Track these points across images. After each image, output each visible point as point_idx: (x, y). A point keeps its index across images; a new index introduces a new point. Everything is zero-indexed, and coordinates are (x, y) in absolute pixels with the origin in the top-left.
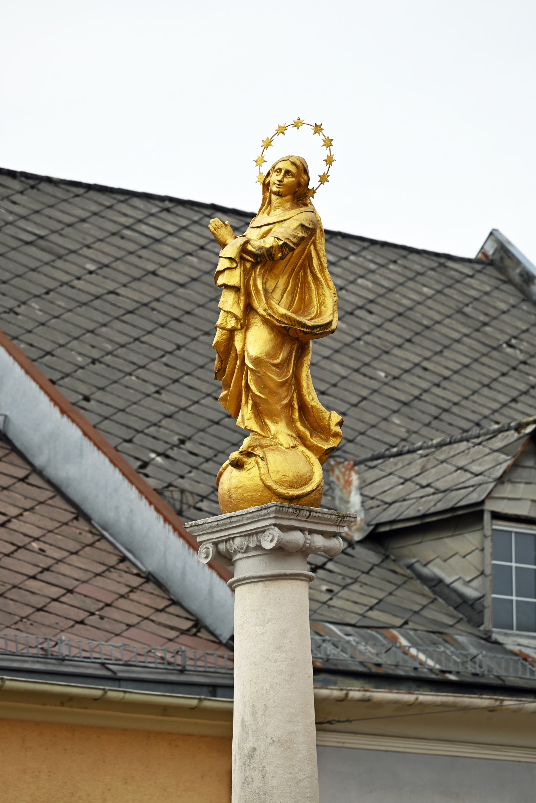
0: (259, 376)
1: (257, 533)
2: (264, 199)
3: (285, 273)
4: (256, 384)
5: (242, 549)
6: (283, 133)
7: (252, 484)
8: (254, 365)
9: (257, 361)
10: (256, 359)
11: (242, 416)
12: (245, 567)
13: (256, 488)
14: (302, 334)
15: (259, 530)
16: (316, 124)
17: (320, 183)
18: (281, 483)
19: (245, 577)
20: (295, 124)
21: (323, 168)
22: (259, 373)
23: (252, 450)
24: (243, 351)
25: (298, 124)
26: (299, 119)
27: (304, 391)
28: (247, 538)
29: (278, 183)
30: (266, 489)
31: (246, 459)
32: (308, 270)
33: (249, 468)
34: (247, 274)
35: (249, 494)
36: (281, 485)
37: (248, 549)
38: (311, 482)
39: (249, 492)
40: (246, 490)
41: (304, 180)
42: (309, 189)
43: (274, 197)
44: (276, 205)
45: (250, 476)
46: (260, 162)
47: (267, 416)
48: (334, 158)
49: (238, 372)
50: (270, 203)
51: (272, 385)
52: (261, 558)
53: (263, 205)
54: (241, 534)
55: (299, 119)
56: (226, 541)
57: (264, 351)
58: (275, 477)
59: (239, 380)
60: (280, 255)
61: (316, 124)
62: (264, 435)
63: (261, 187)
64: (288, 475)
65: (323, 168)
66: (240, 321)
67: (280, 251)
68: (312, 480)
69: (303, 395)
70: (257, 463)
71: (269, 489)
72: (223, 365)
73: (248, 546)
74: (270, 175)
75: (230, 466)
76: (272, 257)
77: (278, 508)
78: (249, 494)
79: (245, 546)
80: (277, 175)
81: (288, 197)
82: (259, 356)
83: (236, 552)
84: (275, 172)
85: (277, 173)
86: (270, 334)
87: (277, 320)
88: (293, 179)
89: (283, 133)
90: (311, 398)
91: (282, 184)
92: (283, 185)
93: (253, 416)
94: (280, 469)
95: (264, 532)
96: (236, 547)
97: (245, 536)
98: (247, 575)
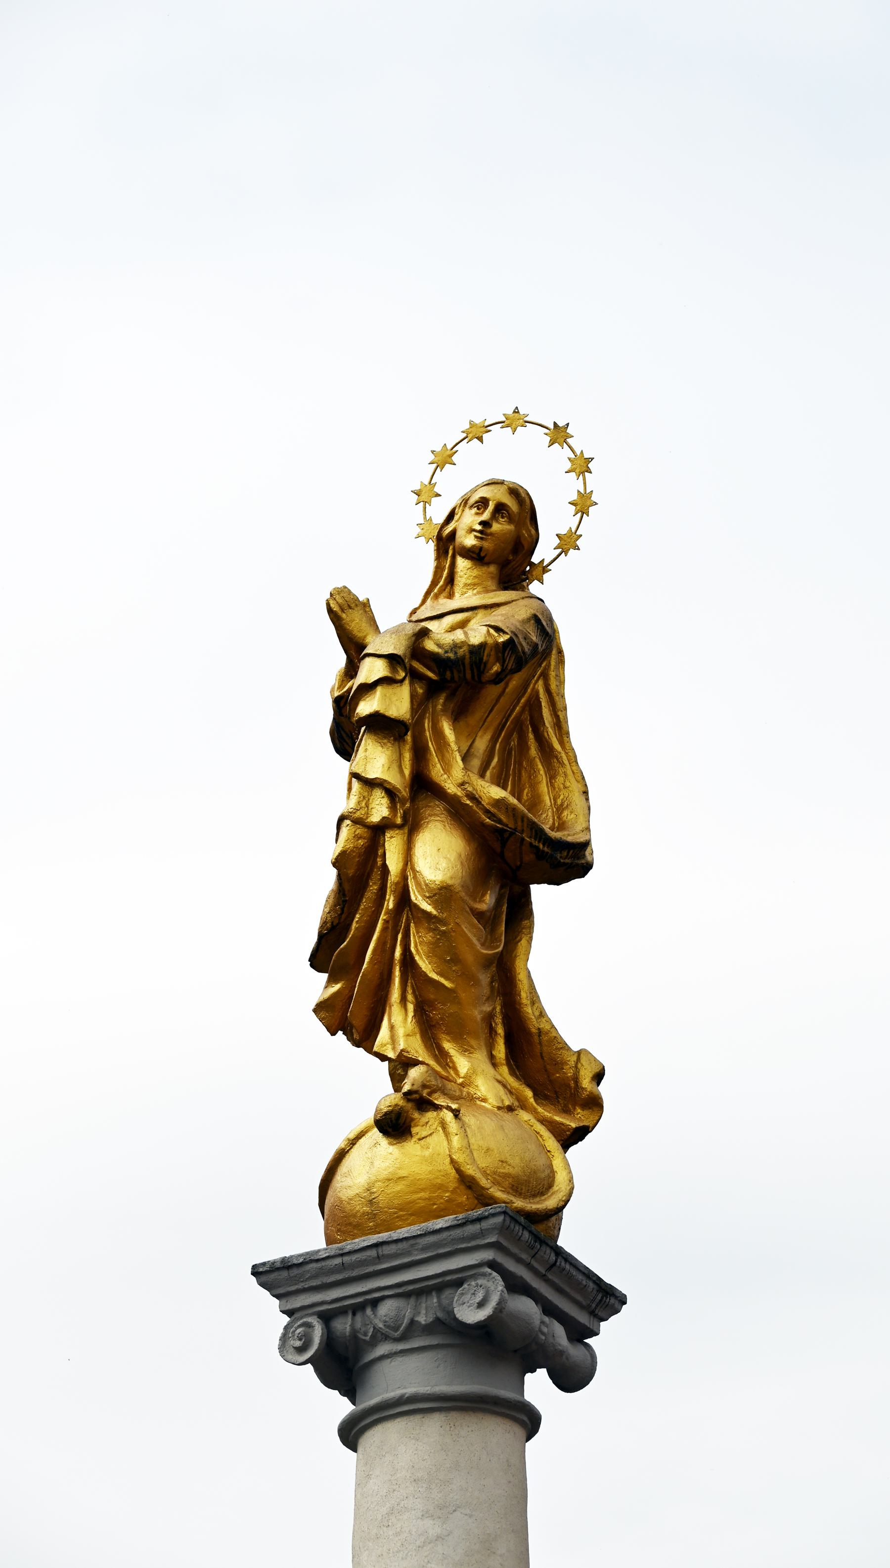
0: (444, 932)
1: (439, 1289)
2: (438, 570)
3: (487, 728)
4: (434, 952)
5: (396, 1329)
6: (480, 439)
7: (430, 1172)
8: (435, 904)
9: (442, 895)
11: (392, 1027)
12: (400, 1374)
13: (439, 1181)
14: (532, 857)
15: (448, 1278)
16: (555, 424)
17: (559, 550)
18: (499, 1179)
19: (402, 1396)
20: (507, 422)
21: (567, 520)
22: (445, 925)
23: (430, 1094)
24: (404, 877)
25: (515, 420)
26: (516, 411)
27: (523, 995)
28: (412, 1300)
29: (479, 528)
30: (462, 1187)
31: (416, 1115)
32: (531, 736)
33: (424, 1134)
34: (418, 705)
35: (422, 1194)
36: (495, 1183)
37: (412, 1329)
38: (551, 1191)
39: (422, 1190)
40: (415, 1185)
41: (530, 535)
42: (532, 565)
43: (462, 564)
44: (469, 582)
45: (427, 1153)
46: (425, 495)
47: (447, 1034)
48: (594, 498)
49: (384, 930)
50: (451, 580)
51: (469, 958)
52: (440, 1354)
53: (434, 583)
54: (400, 1290)
55: (516, 411)
56: (357, 1309)
58: (484, 1162)
59: (385, 949)
60: (496, 668)
61: (555, 424)
62: (444, 1073)
63: (432, 546)
64: (511, 1161)
65: (567, 520)
66: (403, 804)
67: (497, 660)
68: (555, 1188)
69: (520, 1004)
70: (443, 1125)
71: (469, 1187)
72: (344, 916)
73: (412, 1322)
74: (456, 517)
75: (376, 1129)
78: (422, 1194)
79: (406, 1321)
80: (477, 514)
81: (492, 568)
82: (450, 882)
83: (380, 1336)
84: (471, 507)
85: (475, 510)
86: (469, 845)
87: (487, 812)
88: (511, 527)
89: (480, 439)
90: (537, 1013)
91: (489, 531)
92: (491, 534)
93: (417, 1030)
94: (493, 1145)
95: (459, 1283)
96: (381, 1325)
97: (407, 1295)
98: (410, 1390)
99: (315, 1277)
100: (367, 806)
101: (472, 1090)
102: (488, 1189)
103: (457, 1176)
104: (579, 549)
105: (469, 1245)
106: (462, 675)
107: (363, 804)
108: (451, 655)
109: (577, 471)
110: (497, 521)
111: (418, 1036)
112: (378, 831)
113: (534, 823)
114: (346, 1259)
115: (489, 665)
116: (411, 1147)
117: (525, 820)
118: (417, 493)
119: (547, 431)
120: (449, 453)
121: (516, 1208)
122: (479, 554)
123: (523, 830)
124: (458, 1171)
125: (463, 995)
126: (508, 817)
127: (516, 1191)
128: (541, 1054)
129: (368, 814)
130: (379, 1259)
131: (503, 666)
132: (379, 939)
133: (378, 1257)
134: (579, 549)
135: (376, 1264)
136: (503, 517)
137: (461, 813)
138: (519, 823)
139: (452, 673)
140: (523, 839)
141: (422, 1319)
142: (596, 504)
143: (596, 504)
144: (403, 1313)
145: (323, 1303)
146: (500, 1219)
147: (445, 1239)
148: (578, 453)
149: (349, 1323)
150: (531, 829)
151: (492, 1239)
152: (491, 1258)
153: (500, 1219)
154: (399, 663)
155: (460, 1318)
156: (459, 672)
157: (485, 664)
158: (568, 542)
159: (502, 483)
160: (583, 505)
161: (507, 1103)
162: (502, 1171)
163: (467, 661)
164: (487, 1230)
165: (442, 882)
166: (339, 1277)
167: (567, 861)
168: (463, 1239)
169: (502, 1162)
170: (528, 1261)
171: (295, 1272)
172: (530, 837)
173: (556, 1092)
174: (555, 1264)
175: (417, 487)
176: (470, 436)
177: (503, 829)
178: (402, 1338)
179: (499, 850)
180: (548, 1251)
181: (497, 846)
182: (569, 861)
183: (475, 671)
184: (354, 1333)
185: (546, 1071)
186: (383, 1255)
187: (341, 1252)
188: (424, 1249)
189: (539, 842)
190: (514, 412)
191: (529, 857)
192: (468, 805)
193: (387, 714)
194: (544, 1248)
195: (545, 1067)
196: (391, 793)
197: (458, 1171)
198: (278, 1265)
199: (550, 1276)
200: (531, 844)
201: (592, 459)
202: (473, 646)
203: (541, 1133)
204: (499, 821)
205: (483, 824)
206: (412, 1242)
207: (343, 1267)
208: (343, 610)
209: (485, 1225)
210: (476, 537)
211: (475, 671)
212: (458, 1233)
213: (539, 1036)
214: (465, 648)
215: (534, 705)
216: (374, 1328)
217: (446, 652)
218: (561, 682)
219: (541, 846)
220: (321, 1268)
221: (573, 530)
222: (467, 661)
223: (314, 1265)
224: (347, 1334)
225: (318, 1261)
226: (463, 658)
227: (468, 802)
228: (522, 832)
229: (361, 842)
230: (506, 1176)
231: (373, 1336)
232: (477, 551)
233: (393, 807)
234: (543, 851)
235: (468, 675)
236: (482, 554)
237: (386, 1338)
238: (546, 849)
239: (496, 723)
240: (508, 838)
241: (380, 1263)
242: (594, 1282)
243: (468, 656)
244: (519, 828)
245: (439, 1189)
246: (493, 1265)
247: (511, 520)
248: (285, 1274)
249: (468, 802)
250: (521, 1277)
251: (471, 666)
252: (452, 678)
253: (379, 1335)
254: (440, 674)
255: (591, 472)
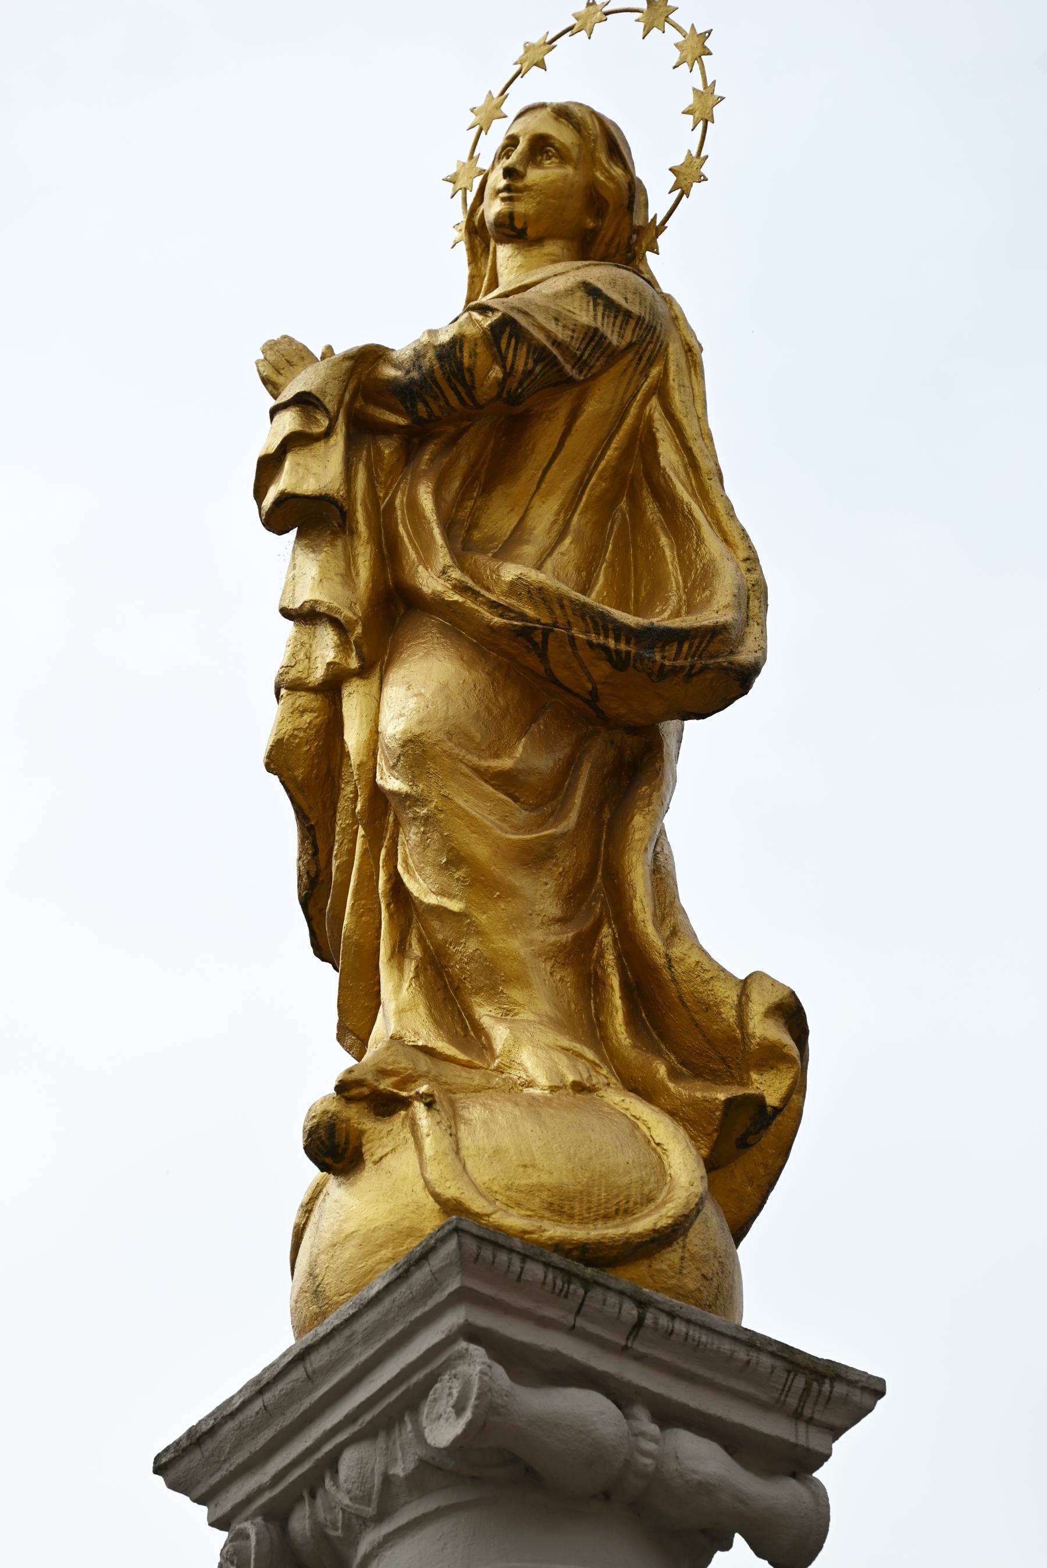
3: (550, 493)
6: (541, 64)
7: (391, 1212)
10: (403, 746)
31: (369, 1125)
39: (381, 1246)
51: (481, 851)
54: (356, 1428)
57: (441, 715)
73: (387, 1480)
76: (464, 385)
77: (471, 1245)
79: (377, 1480)
82: (417, 731)
86: (470, 665)
89: (541, 64)
92: (527, 188)
99: (238, 1446)
100: (308, 658)
101: (515, 1074)
102: (488, 1215)
103: (438, 1207)
104: (706, 179)
105: (426, 1309)
106: (442, 403)
107: (302, 656)
108: (415, 374)
109: (689, 58)
110: (539, 165)
111: (422, 1010)
112: (331, 689)
113: (584, 605)
114: (268, 1397)
115: (479, 373)
116: (369, 1178)
117: (565, 602)
118: (452, 180)
119: (638, 15)
120: (495, 102)
121: (551, 1238)
122: (512, 226)
123: (569, 622)
124: (436, 1197)
125: (483, 918)
126: (535, 606)
127: (560, 1212)
128: (680, 997)
129: (310, 670)
130: (312, 1379)
131: (504, 367)
132: (359, 870)
133: (309, 1378)
134: (706, 179)
135: (310, 1392)
136: (549, 158)
137: (454, 623)
138: (558, 612)
139: (427, 405)
140: (572, 638)
141: (399, 1470)
142: (723, 98)
143: (723, 98)
144: (370, 1466)
145: (260, 1491)
146: (452, 1245)
147: (389, 1311)
148: (688, 30)
149: (307, 1513)
150: (583, 617)
151: (454, 1284)
152: (462, 1321)
153: (452, 1245)
154: (316, 407)
155: (432, 1443)
156: (436, 398)
157: (471, 370)
158: (686, 177)
159: (543, 106)
160: (703, 109)
161: (571, 1078)
162: (523, 1182)
163: (439, 375)
164: (441, 1270)
165: (404, 732)
166: (268, 1435)
167: (680, 662)
168: (415, 1301)
169: (525, 1166)
170: (570, 1320)
171: (210, 1446)
172: (587, 632)
173: (723, 1060)
174: (640, 1323)
175: (452, 170)
176: (526, 65)
177: (525, 628)
178: (382, 1515)
179: (541, 669)
180: (612, 1299)
181: (532, 661)
182: (717, 671)
183: (460, 388)
184: (319, 1531)
185: (697, 1025)
186: (314, 1372)
187: (258, 1387)
188: (368, 1338)
189: (606, 637)
190: (589, 4)
191: (602, 670)
192: (456, 602)
193: (298, 491)
194: (597, 1293)
195: (693, 1019)
196: (339, 626)
197: (436, 1197)
198: (184, 1444)
199: (638, 1347)
200: (590, 643)
201: (710, 32)
202: (442, 346)
203: (644, 1117)
204: (522, 616)
205: (492, 629)
206: (347, 1332)
207: (269, 1414)
208: (278, 372)
209: (436, 1261)
210: (503, 199)
211: (460, 388)
212: (403, 1292)
213: (670, 967)
214: (431, 354)
215: (643, 443)
216: (344, 1511)
217: (408, 372)
218: (698, 399)
219: (612, 643)
220: (240, 1427)
221: (694, 153)
222: (439, 375)
223: (231, 1425)
224: (308, 1534)
225: (232, 1415)
226: (431, 370)
227: (456, 597)
228: (569, 626)
229: (307, 717)
230: (531, 1191)
231: (347, 1526)
232: (507, 222)
233: (343, 645)
234: (618, 652)
235: (454, 401)
236: (519, 225)
237: (367, 1523)
238: (623, 647)
239: (568, 483)
240: (545, 642)
241: (316, 1387)
242: (773, 1354)
243: (437, 367)
244: (561, 621)
245: (408, 1236)
246: (471, 1333)
247: (563, 156)
248: (197, 1456)
249: (456, 597)
250: (557, 1353)
251: (449, 380)
252: (431, 413)
253: (354, 1521)
254: (410, 412)
255: (710, 54)
